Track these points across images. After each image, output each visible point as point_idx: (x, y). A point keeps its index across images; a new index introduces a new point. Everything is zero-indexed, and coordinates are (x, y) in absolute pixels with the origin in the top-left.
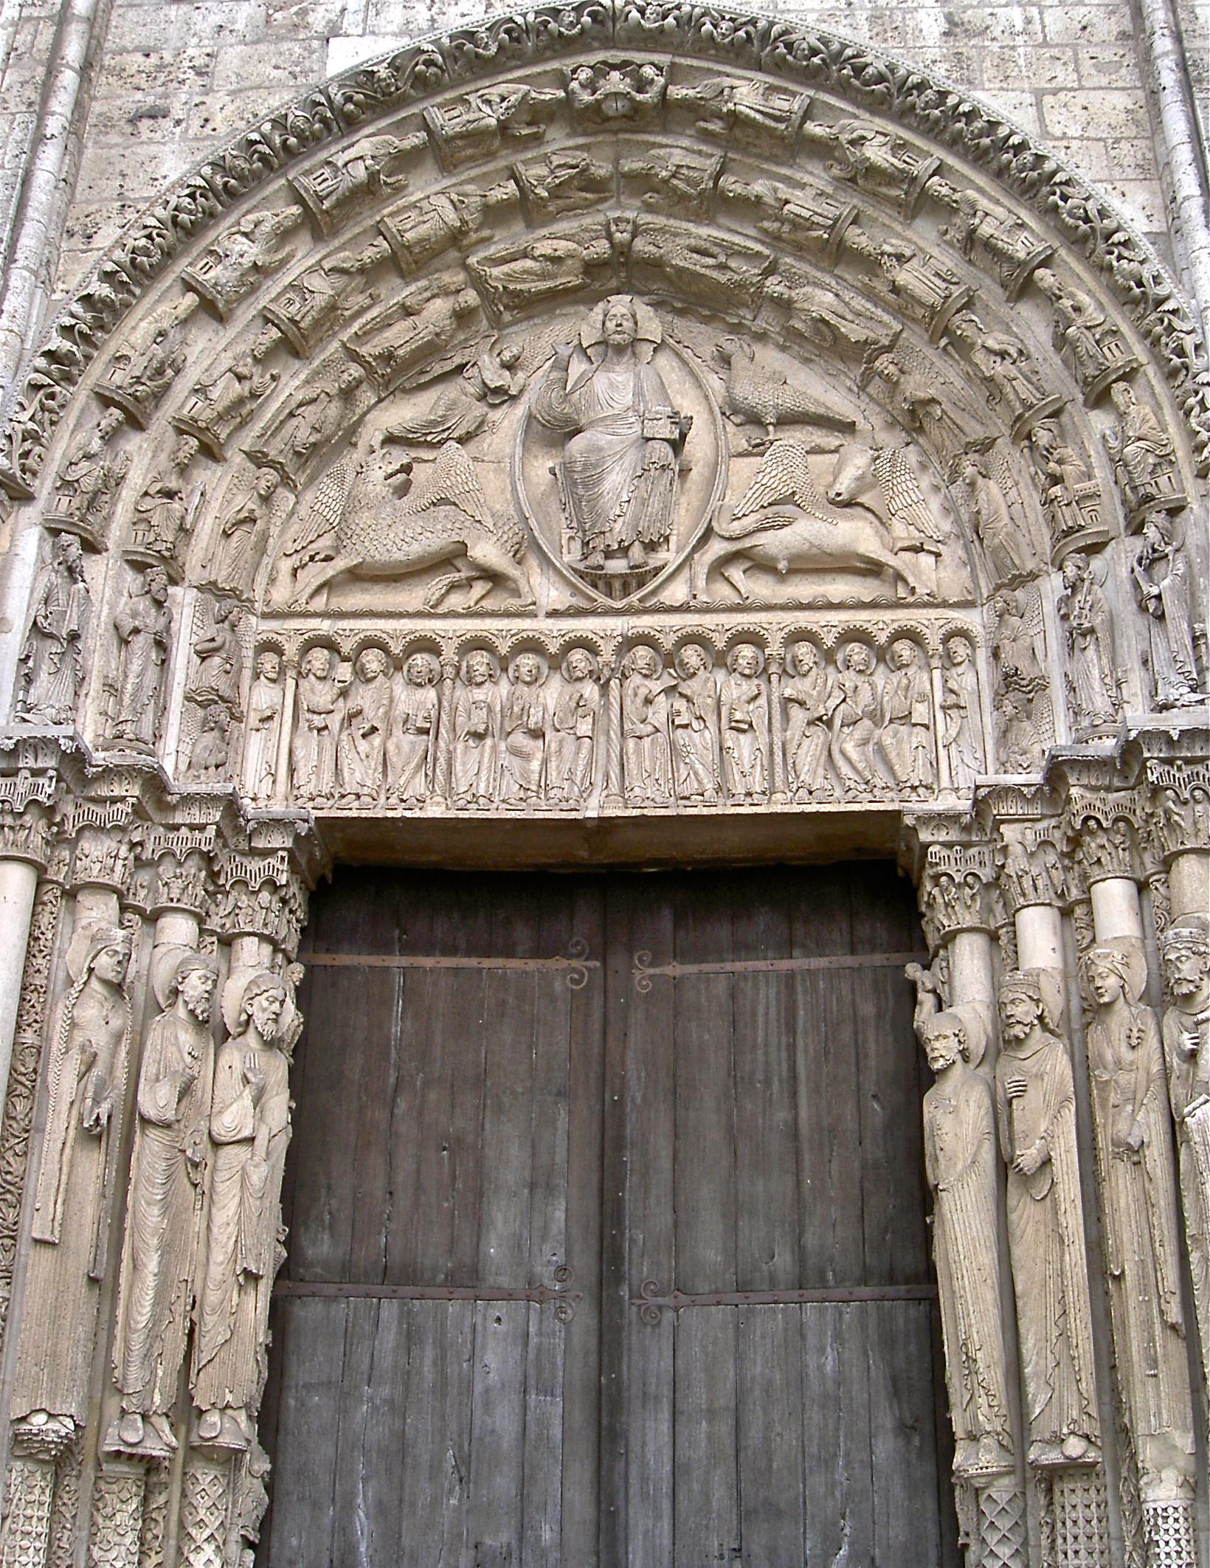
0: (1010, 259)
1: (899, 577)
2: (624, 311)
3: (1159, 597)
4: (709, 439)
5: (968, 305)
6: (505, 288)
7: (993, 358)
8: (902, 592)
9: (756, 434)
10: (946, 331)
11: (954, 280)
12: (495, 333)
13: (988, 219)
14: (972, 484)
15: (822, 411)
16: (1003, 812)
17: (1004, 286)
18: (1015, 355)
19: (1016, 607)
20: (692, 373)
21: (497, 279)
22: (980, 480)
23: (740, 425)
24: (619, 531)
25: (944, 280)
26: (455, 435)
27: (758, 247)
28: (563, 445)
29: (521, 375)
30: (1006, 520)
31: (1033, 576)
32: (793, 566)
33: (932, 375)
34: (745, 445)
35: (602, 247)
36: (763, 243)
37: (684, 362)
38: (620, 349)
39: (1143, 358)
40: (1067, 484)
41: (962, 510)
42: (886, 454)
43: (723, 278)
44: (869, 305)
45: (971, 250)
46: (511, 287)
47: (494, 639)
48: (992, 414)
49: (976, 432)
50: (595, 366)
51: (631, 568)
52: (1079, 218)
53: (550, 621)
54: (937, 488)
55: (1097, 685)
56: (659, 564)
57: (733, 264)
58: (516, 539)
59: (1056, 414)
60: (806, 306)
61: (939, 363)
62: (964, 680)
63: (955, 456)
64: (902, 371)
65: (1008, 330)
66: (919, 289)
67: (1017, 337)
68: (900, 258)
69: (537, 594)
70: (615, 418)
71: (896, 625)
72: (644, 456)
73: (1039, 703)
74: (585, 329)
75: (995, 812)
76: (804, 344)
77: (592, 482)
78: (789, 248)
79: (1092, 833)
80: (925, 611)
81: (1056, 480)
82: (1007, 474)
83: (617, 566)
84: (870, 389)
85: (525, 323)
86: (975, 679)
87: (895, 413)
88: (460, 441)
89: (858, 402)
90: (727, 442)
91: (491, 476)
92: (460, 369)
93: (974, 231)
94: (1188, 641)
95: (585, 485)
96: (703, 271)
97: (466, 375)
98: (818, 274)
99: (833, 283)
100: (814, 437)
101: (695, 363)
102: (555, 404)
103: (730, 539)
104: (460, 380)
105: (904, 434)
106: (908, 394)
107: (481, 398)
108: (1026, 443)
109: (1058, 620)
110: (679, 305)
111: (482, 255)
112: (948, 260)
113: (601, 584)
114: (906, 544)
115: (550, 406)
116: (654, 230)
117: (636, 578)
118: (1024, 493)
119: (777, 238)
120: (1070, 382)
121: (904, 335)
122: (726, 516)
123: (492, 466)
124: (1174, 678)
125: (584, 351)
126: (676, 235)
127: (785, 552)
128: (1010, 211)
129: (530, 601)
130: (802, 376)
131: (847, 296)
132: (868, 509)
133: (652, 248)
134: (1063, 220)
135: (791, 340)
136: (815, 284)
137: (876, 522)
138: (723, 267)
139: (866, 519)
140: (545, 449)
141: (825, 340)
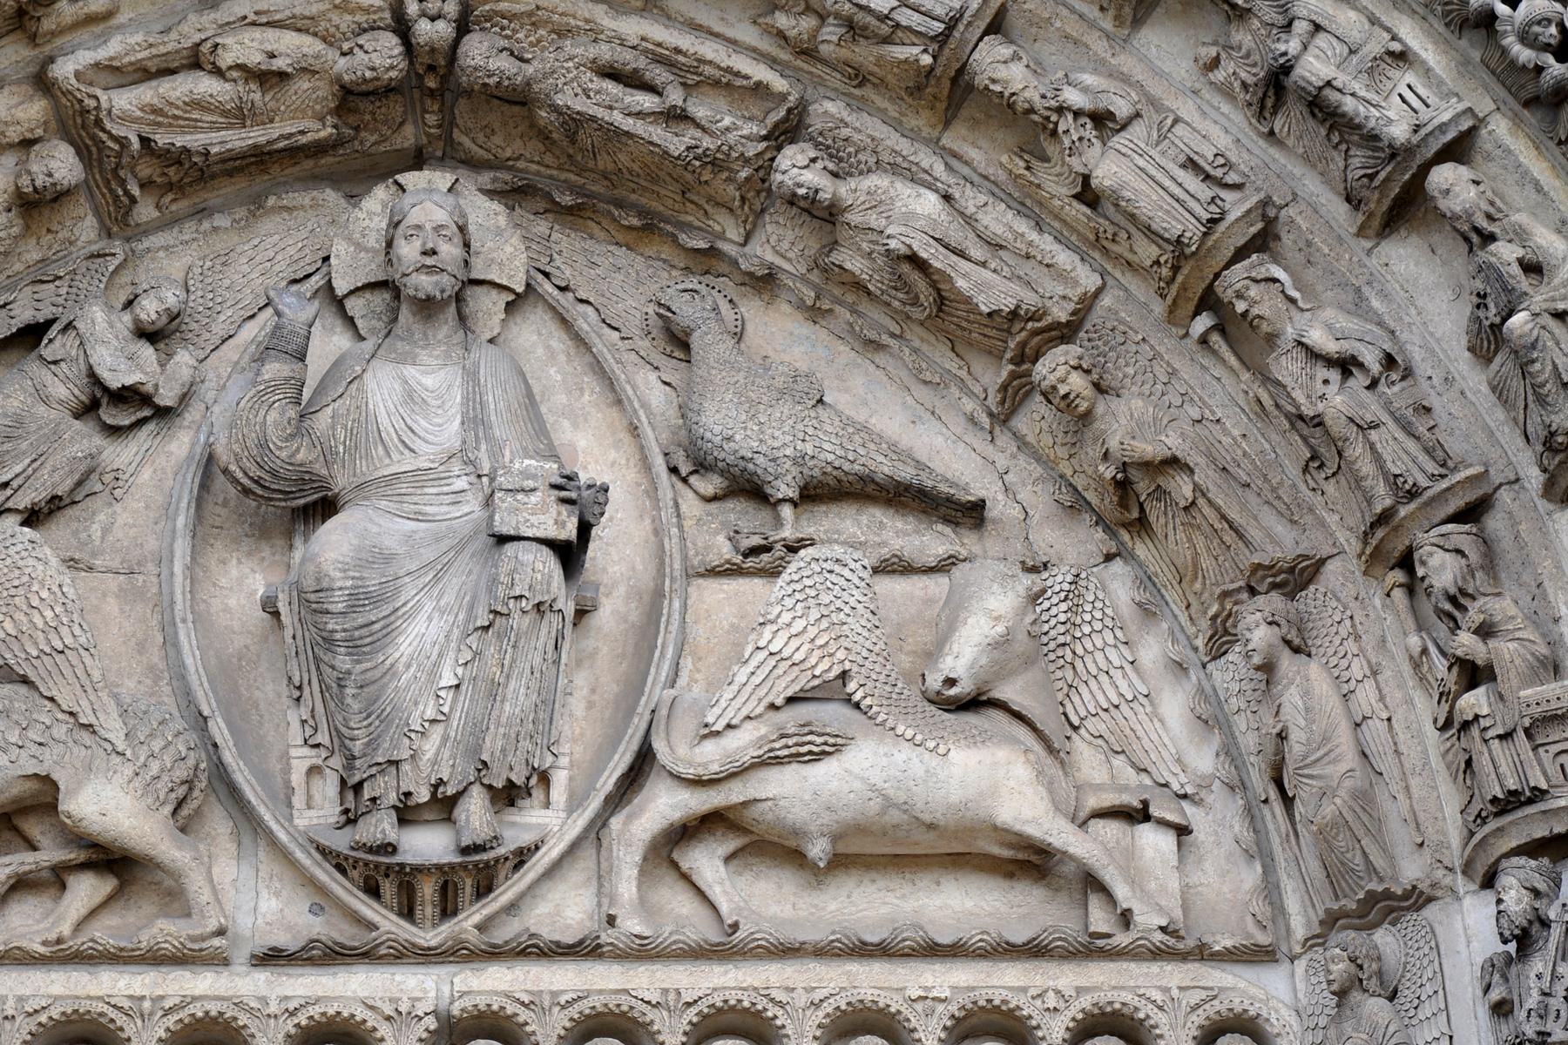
0: (1371, 138)
1: (1092, 883)
2: (441, 216)
4: (640, 531)
5: (1263, 241)
6: (145, 141)
7: (1322, 373)
8: (1100, 918)
9: (747, 519)
10: (1209, 301)
11: (1232, 178)
12: (118, 247)
13: (1322, 40)
14: (1268, 668)
15: (905, 473)
17: (1352, 199)
18: (1376, 368)
19: (1380, 973)
20: (599, 369)
21: (125, 118)
22: (1287, 662)
23: (714, 498)
24: (433, 759)
25: (1207, 177)
26: (23, 501)
27: (760, 72)
28: (289, 535)
29: (184, 359)
30: (1350, 759)
31: (1418, 899)
32: (841, 849)
33: (1169, 400)
34: (723, 550)
35: (381, 55)
36: (772, 62)
37: (580, 341)
38: (427, 307)
40: (1502, 686)
41: (1241, 723)
42: (1059, 579)
43: (676, 142)
44: (1022, 226)
45: (1274, 114)
46: (162, 139)
47: (121, 1020)
49: (1278, 540)
50: (368, 346)
51: (465, 851)
52: (1546, 48)
53: (262, 976)
56: (526, 839)
57: (700, 111)
58: (181, 773)
59: (1472, 513)
60: (874, 220)
61: (1186, 371)
63: (1225, 594)
64: (1098, 387)
65: (1358, 305)
66: (1149, 202)
67: (1380, 324)
68: (1102, 120)
69: (229, 907)
70: (420, 477)
71: (1086, 1002)
72: (494, 580)
74: (341, 251)
76: (865, 306)
77: (368, 640)
78: (835, 80)
80: (1155, 968)
81: (1473, 674)
82: (1351, 646)
83: (427, 845)
84: (1021, 423)
85: (189, 228)
87: (1079, 482)
88: (33, 518)
89: (989, 450)
90: (683, 539)
91: (112, 606)
92: (32, 336)
93: (1286, 69)
95: (355, 647)
96: (628, 124)
97: (48, 352)
98: (904, 146)
99: (939, 169)
100: (888, 535)
101: (604, 342)
102: (274, 436)
103: (698, 783)
104: (33, 367)
105: (1099, 534)
106: (1113, 444)
107: (87, 411)
108: (1398, 576)
109: (1483, 1012)
110: (567, 200)
111: (85, 58)
112: (1220, 129)
113: (388, 888)
114: (1109, 799)
115: (263, 445)
116: (511, 17)
117: (479, 871)
118: (1394, 696)
119: (807, 52)
120: (1510, 438)
121: (1106, 301)
122: (685, 726)
123: (113, 582)
125: (339, 303)
126: (562, 32)
127: (827, 818)
128: (1374, 21)
129: (212, 925)
130: (858, 382)
131: (971, 199)
132: (1018, 716)
133: (504, 64)
134: (1504, 52)
135: (832, 294)
136: (895, 169)
137: (1038, 748)
138: (675, 116)
139: (1015, 741)
140: (247, 544)
141: (915, 302)
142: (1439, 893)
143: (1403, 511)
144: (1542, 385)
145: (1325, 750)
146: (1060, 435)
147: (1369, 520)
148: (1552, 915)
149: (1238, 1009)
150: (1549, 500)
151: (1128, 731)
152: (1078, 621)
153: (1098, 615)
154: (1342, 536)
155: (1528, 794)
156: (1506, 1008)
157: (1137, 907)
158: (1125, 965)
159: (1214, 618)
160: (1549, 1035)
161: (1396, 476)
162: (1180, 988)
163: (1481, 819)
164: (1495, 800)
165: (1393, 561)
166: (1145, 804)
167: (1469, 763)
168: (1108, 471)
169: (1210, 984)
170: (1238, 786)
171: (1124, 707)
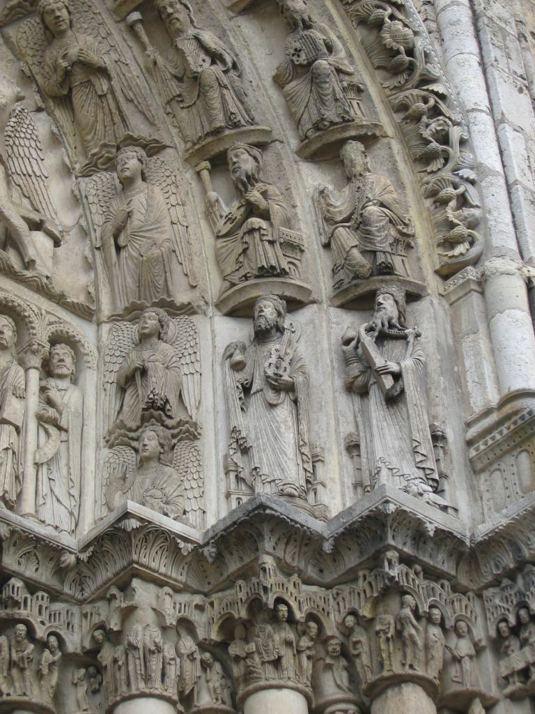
3: (397, 376)
7: (202, 56)
16: (144, 561)
18: (230, 65)
22: (139, 182)
31: (189, 310)
39: (389, 130)
48: (168, 119)
49: (140, 128)
54: (67, 171)
55: (290, 450)
62: (67, 396)
63: (105, 146)
65: (223, 35)
73: (183, 450)
75: (135, 557)
79: (274, 618)
80: (36, 296)
86: (89, 400)
94: (430, 437)
105: (37, 97)
108: (207, 164)
118: (191, 219)
124: (409, 469)
142: (200, 312)
143: (227, 132)
144: (326, 95)
145: (156, 226)
146: (32, 44)
147: (207, 129)
148: (286, 327)
149: (71, 334)
150: (299, 156)
151: (33, 189)
152: (19, 129)
153: (30, 132)
154: (177, 140)
155: (279, 271)
156: (238, 367)
157: (38, 262)
158: (22, 288)
159: (93, 155)
160: (281, 376)
161: (232, 113)
162: (46, 312)
163: (246, 277)
164: (262, 268)
165: (208, 156)
166: (42, 222)
167: (245, 251)
168: (64, 64)
169: (60, 316)
170: (85, 233)
171: (33, 177)
